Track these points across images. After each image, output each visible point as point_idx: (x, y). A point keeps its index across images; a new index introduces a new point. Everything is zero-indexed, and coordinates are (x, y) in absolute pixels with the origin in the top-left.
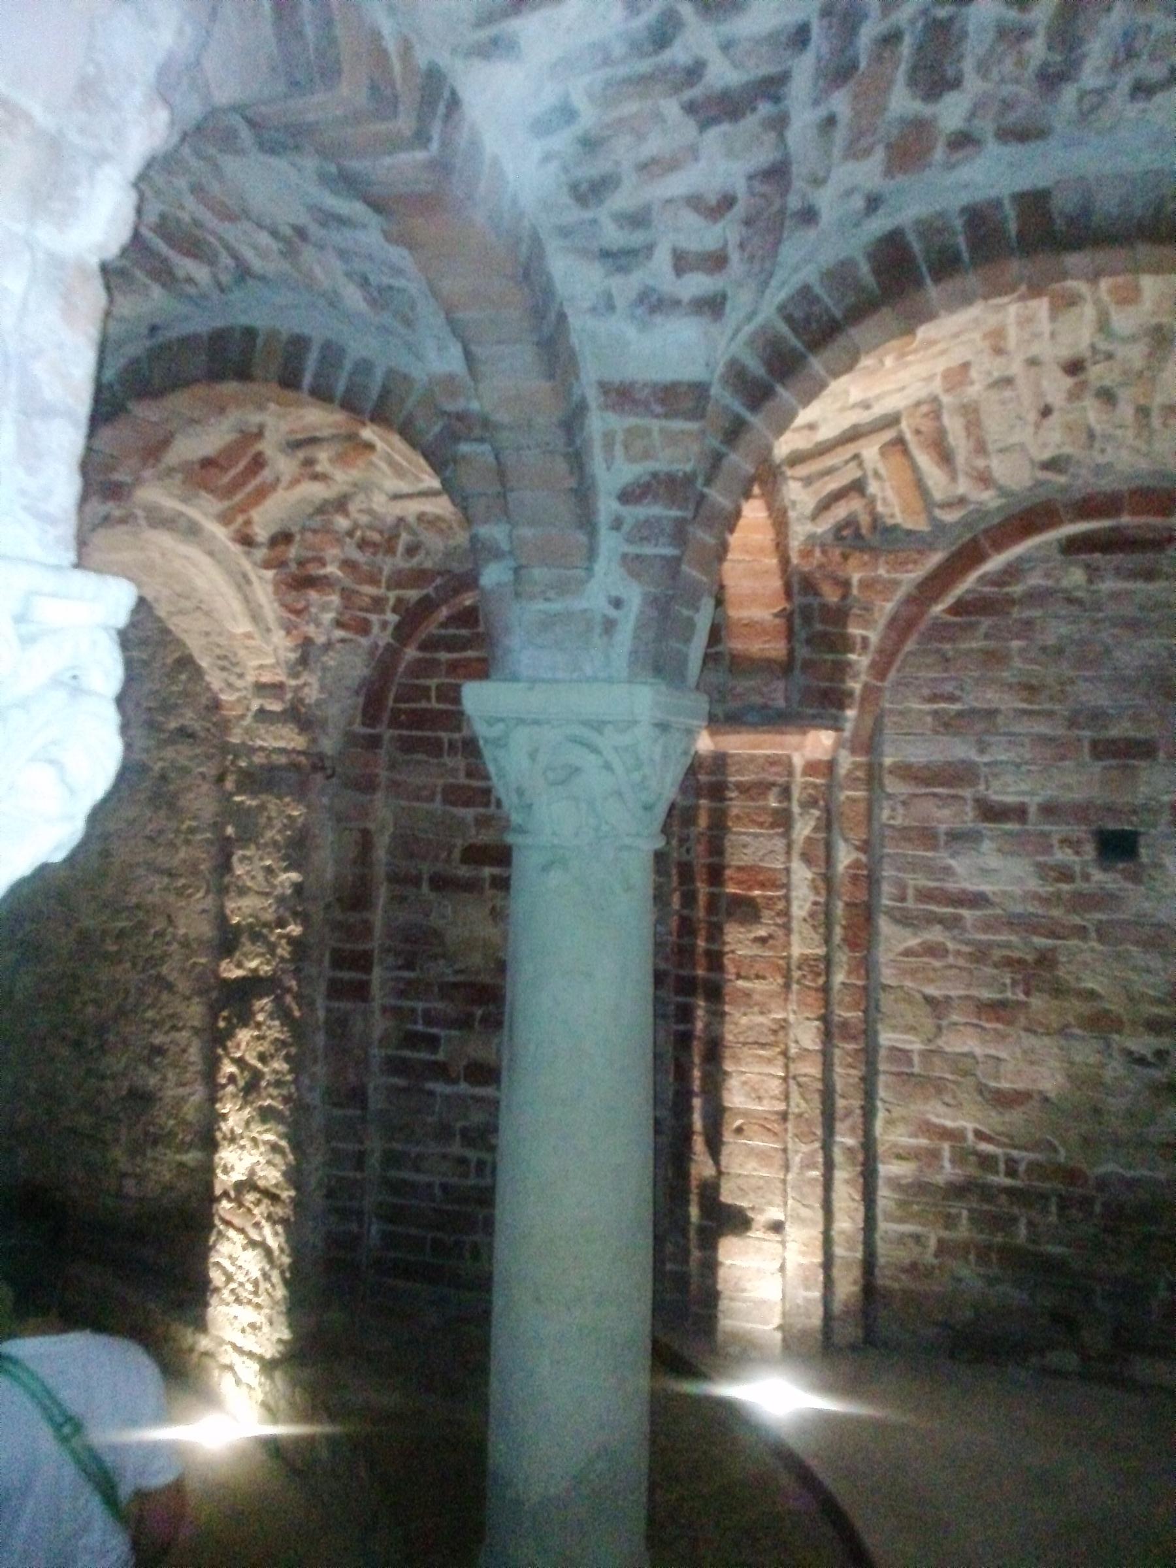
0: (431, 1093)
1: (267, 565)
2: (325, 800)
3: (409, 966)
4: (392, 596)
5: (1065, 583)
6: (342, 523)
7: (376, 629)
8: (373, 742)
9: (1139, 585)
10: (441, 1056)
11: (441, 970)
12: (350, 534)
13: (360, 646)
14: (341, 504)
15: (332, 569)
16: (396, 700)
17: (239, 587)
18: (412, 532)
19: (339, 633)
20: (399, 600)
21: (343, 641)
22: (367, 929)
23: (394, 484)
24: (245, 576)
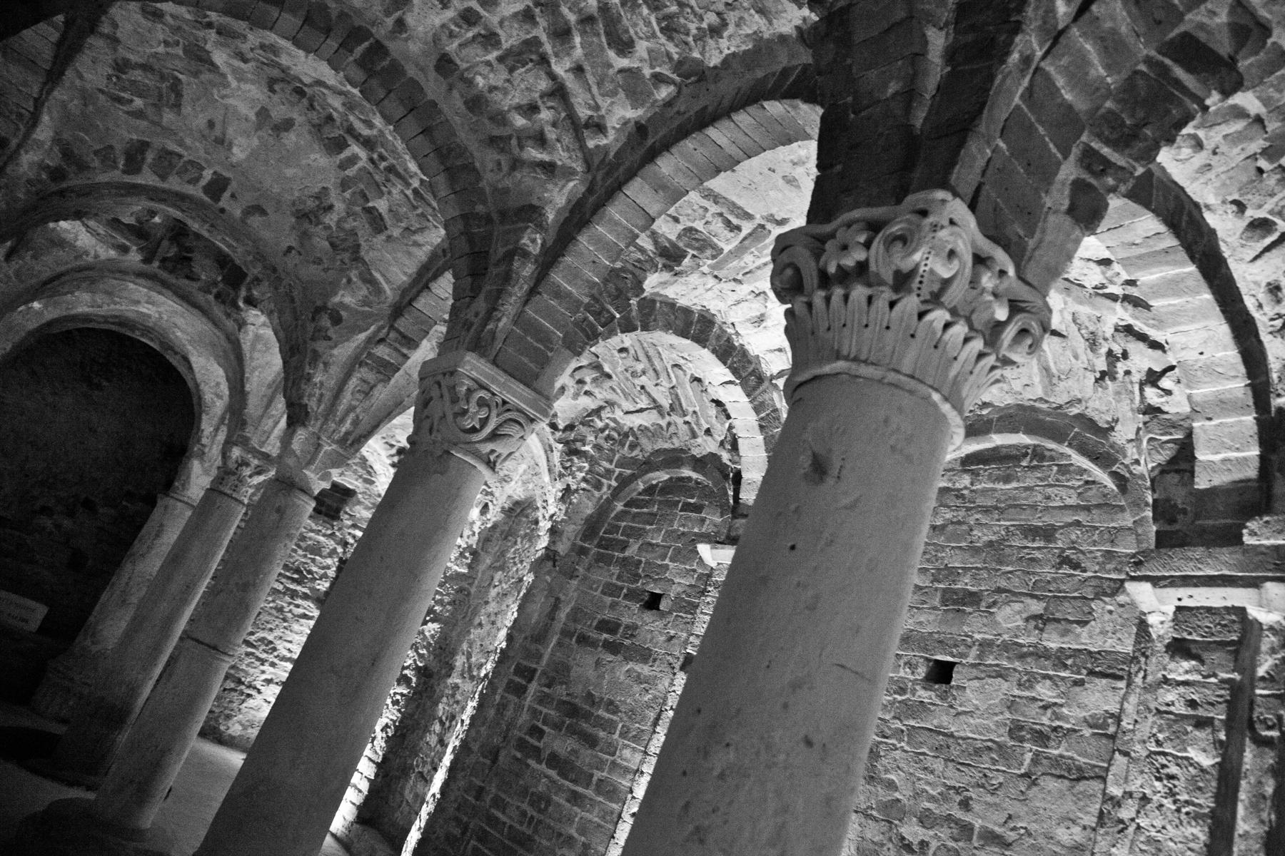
0: (528, 766)
1: (559, 441)
2: (548, 578)
3: (549, 686)
4: (618, 470)
5: (958, 486)
6: (600, 424)
7: (605, 489)
8: (583, 551)
9: (1000, 486)
10: (541, 745)
11: (560, 691)
12: (602, 430)
13: (593, 495)
14: (597, 412)
15: (587, 448)
16: (605, 533)
17: (546, 451)
18: (634, 435)
19: (583, 485)
20: (620, 474)
21: (584, 489)
22: (540, 656)
23: (628, 406)
24: (550, 446)
